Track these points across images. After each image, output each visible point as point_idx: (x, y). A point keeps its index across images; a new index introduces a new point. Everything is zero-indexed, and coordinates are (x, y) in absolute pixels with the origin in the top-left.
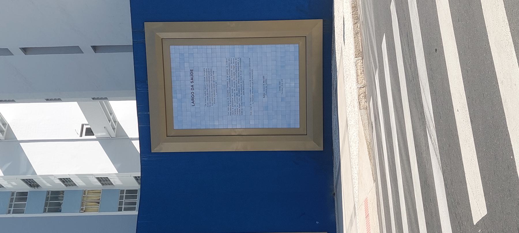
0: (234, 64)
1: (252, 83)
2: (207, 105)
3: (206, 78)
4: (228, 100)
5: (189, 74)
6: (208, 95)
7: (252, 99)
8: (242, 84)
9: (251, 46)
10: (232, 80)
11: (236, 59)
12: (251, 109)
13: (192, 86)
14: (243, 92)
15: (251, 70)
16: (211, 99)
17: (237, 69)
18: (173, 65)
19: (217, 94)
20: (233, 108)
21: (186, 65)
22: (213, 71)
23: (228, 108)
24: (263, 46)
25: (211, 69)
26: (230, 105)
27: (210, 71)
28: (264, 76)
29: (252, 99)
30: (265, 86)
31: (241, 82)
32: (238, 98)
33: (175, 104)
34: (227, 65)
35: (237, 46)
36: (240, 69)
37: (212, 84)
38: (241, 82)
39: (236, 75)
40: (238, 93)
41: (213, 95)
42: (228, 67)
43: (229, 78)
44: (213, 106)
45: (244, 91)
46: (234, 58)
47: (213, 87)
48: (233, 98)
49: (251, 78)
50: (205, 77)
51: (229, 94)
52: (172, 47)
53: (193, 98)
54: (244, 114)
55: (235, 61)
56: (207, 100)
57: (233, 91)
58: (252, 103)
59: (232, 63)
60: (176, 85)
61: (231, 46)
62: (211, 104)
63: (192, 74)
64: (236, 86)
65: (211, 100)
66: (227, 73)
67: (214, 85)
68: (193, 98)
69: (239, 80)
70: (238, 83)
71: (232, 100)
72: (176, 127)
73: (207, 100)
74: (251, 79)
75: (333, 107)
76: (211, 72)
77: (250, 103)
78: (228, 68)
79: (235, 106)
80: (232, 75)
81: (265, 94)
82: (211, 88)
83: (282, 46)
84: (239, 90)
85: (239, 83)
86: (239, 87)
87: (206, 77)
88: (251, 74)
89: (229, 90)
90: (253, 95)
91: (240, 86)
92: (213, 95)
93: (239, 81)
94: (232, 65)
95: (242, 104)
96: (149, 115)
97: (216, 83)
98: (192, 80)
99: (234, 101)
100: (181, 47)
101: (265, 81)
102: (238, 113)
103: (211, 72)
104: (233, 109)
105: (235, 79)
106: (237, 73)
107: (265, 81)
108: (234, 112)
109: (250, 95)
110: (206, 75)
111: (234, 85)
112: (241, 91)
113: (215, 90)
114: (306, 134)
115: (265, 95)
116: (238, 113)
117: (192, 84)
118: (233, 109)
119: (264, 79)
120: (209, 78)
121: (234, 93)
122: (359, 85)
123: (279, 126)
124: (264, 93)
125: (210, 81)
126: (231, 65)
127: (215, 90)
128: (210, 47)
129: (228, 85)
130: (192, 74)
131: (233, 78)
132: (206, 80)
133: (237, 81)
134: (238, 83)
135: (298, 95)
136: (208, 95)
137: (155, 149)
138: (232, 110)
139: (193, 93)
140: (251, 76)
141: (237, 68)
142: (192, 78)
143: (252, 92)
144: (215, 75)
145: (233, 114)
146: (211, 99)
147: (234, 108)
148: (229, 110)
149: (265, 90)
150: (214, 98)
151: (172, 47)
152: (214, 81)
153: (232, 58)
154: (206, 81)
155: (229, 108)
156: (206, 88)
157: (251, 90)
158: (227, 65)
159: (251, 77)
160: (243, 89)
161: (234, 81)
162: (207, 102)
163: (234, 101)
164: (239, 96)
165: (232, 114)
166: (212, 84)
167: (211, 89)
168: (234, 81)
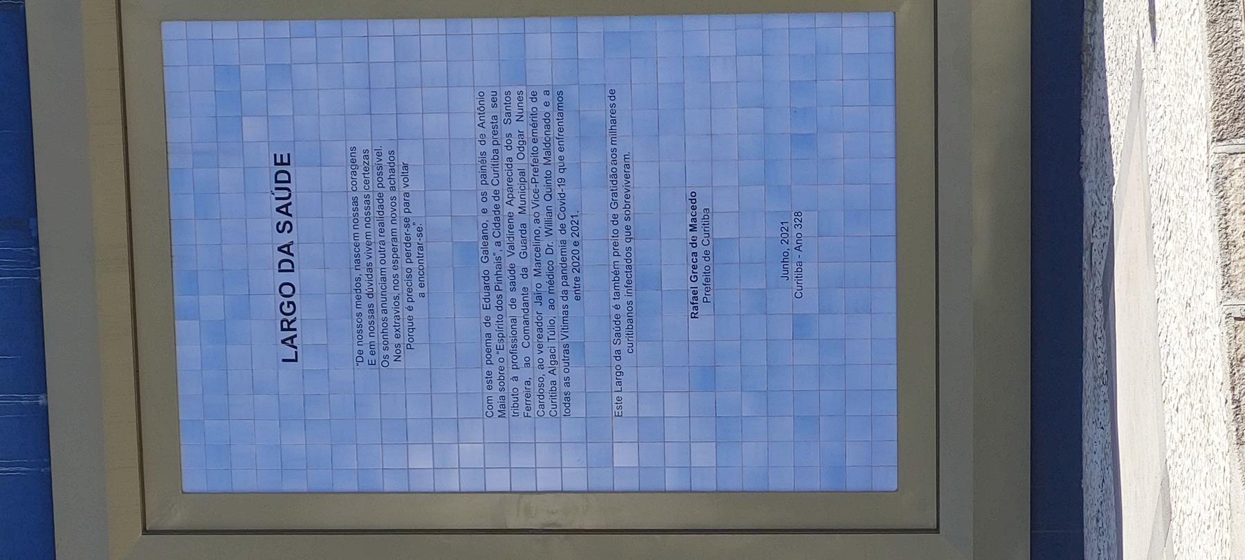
0: (524, 126)
2: (367, 355)
3: (362, 205)
4: (486, 330)
5: (267, 182)
6: (373, 301)
7: (624, 325)
8: (567, 237)
9: (621, 24)
11: (534, 94)
12: (619, 383)
13: (285, 249)
14: (571, 281)
15: (620, 159)
16: (391, 322)
17: (542, 154)
18: (180, 130)
19: (422, 295)
21: (253, 128)
22: (406, 166)
23: (489, 373)
26: (501, 360)
27: (385, 161)
28: (694, 194)
29: (624, 325)
30: (700, 250)
31: (563, 227)
32: (547, 315)
33: (189, 351)
34: (481, 131)
35: (543, 22)
37: (395, 239)
38: (563, 227)
40: (545, 287)
41: (404, 303)
43: (491, 203)
44: (400, 365)
45: (577, 279)
46: (523, 89)
47: (402, 253)
48: (514, 320)
49: (622, 203)
50: (355, 201)
51: (494, 295)
53: (290, 318)
55: (528, 106)
56: (366, 331)
57: (519, 279)
58: (624, 345)
59: (514, 118)
61: (505, 25)
62: (392, 352)
63: (282, 182)
64: (531, 250)
65: (391, 331)
66: (484, 176)
68: (290, 318)
69: (549, 212)
70: (543, 234)
71: (508, 332)
72: (193, 481)
73: (366, 331)
74: (620, 212)
75: (1088, 374)
76: (392, 170)
77: (617, 347)
78: (489, 148)
79: (527, 364)
80: (510, 189)
81: (701, 295)
82: (389, 259)
83: (799, 22)
84: (551, 274)
85: (549, 233)
86: (550, 258)
87: (361, 201)
88: (621, 179)
89: (493, 271)
91: (558, 250)
92: (404, 303)
93: (549, 223)
94: (514, 128)
95: (567, 351)
96: (45, 409)
97: (420, 230)
98: (287, 213)
99: (520, 335)
100: (226, 30)
101: (699, 220)
102: (542, 406)
103: (392, 170)
104: (515, 378)
105: (529, 210)
106: (542, 173)
107: (699, 220)
108: (522, 398)
109: (614, 303)
110: (360, 185)
112: (565, 277)
114: (933, 525)
115: (700, 303)
116: (542, 406)
117: (285, 238)
118: (515, 378)
119: (694, 208)
120: (381, 206)
121: (519, 287)
122: (1234, 301)
123: (784, 480)
124: (695, 293)
125: (387, 222)
126: (505, 129)
129: (485, 245)
130: (282, 182)
131: (517, 202)
132: (362, 213)
133: (537, 221)
134: (543, 234)
135: (887, 302)
136: (373, 301)
139: (287, 290)
141: (540, 145)
142: (286, 206)
143: (623, 282)
144: (416, 184)
146: (391, 322)
147: (524, 374)
148: (496, 384)
150: (410, 319)
153: (514, 91)
154: (362, 223)
155: (496, 376)
156: (364, 260)
159: (621, 199)
161: (523, 219)
162: (367, 340)
163: (520, 335)
164: (552, 306)
165: (509, 411)
166: (395, 239)
167: (389, 264)
168: (523, 219)
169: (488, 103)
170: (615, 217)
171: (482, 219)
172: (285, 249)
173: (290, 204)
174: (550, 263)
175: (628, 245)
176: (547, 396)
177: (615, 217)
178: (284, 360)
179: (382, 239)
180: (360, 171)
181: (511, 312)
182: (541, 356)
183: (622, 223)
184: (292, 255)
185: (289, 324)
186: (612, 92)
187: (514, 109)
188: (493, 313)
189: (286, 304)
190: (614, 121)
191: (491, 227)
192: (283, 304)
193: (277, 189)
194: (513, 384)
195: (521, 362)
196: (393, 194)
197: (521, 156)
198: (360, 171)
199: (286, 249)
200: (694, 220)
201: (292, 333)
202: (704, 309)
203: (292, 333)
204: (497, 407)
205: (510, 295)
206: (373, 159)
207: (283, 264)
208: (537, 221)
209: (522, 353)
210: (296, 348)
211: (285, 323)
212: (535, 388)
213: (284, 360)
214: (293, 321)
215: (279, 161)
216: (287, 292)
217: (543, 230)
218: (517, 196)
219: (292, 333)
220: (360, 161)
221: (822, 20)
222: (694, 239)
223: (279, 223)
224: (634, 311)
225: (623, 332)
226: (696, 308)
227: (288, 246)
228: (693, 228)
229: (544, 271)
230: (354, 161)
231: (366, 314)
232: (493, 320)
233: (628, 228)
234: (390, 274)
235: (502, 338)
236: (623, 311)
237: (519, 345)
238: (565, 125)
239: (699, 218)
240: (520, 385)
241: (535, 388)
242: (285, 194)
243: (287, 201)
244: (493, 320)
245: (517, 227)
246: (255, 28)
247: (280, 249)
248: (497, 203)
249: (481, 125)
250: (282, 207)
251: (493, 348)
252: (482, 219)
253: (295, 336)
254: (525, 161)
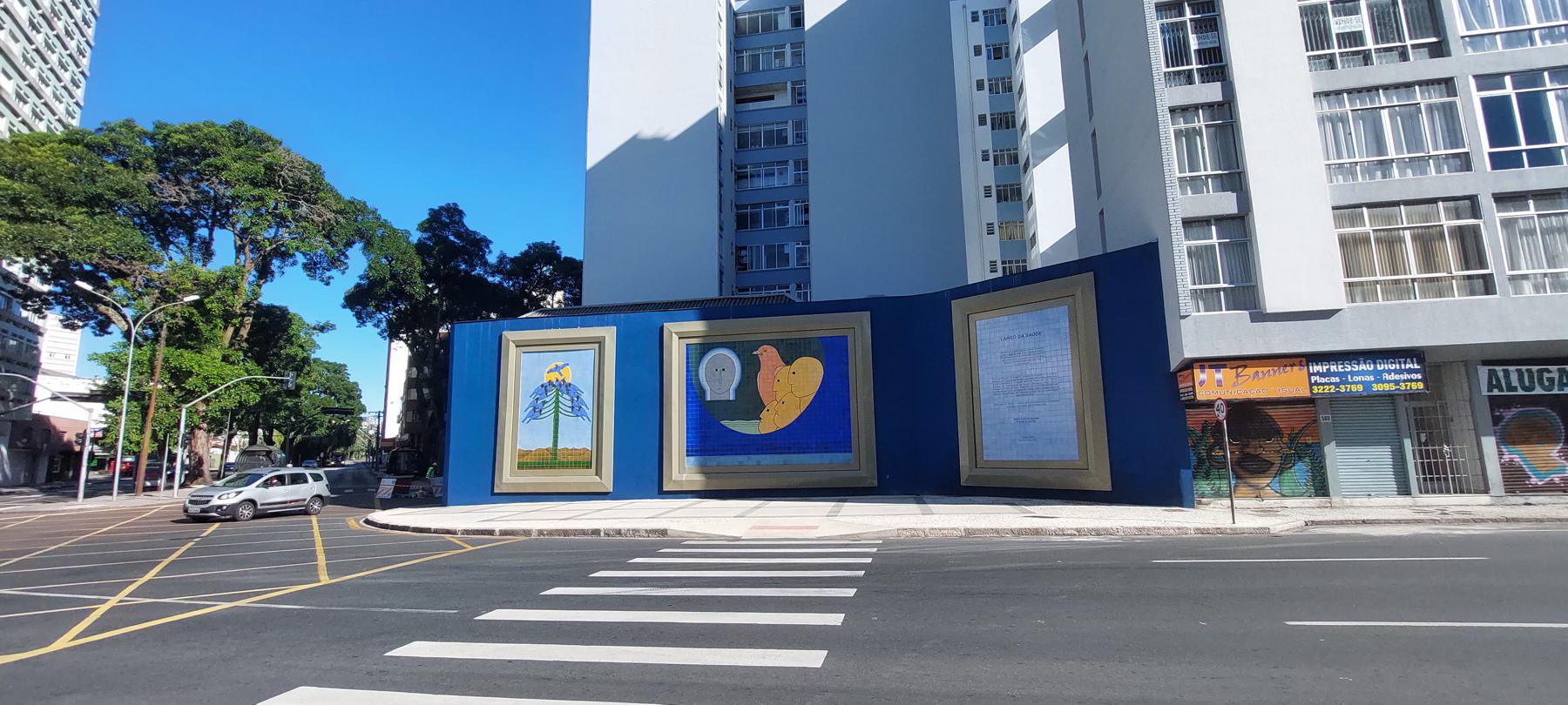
107: (1033, 420)
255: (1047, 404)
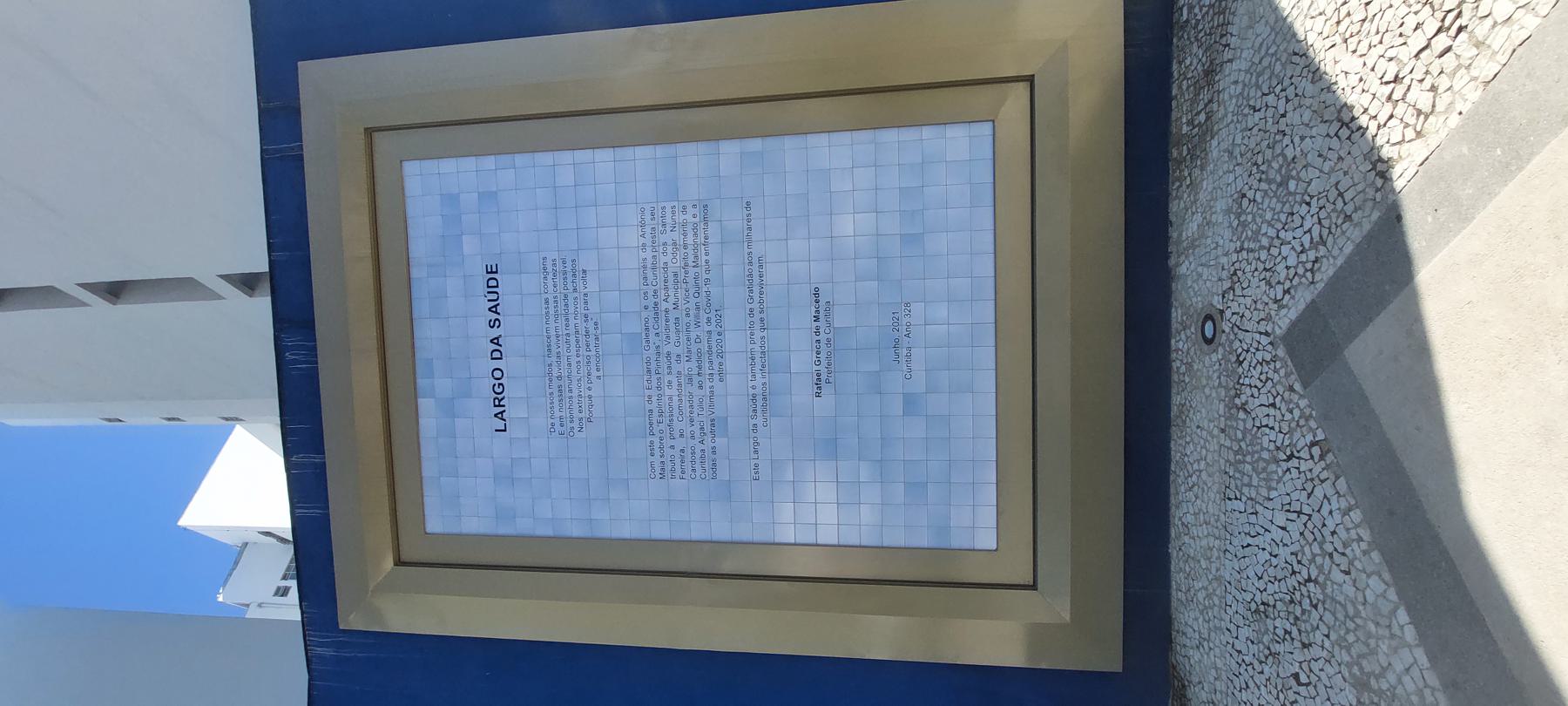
0: (676, 236)
1: (757, 326)
3: (551, 305)
4: (648, 407)
5: (481, 288)
6: (562, 383)
9: (755, 145)
10: (667, 311)
12: (756, 452)
13: (495, 341)
14: (716, 366)
15: (755, 260)
16: (575, 400)
17: (691, 258)
18: (420, 248)
19: (599, 377)
20: (672, 442)
21: (469, 245)
22: (584, 271)
23: (652, 442)
24: (813, 140)
25: (573, 261)
26: (661, 431)
27: (569, 269)
30: (823, 337)
31: (709, 320)
33: (429, 421)
34: (642, 240)
35: (692, 147)
36: (704, 258)
37: (577, 332)
38: (709, 320)
39: (684, 286)
40: (695, 371)
41: (584, 383)
42: (649, 249)
43: (652, 300)
44: (582, 435)
45: (721, 364)
46: (676, 203)
47: (582, 343)
48: (671, 398)
49: (757, 299)
50: (547, 302)
51: (654, 378)
52: (411, 168)
53: (500, 397)
54: (723, 474)
58: (759, 421)
59: (668, 228)
60: (430, 334)
61: (661, 151)
62: (576, 425)
63: (492, 288)
64: (683, 338)
65: (575, 407)
67: (587, 334)
68: (500, 397)
72: (434, 525)
73: (556, 409)
74: (756, 306)
76: (574, 275)
77: (754, 422)
78: (649, 254)
79: (682, 436)
80: (666, 288)
81: (823, 377)
82: (573, 349)
83: (908, 135)
85: (697, 325)
86: (699, 346)
89: (654, 358)
90: (766, 380)
91: (704, 338)
93: (697, 316)
94: (668, 237)
95: (713, 425)
97: (596, 324)
98: (496, 312)
99: (676, 412)
100: (448, 166)
101: (821, 310)
102: (694, 470)
103: (574, 275)
105: (682, 306)
107: (821, 310)
108: (678, 461)
109: (751, 384)
111: (678, 331)
113: (593, 360)
116: (694, 470)
117: (495, 332)
120: (566, 305)
121: (674, 371)
125: (571, 317)
127: (593, 360)
128: (566, 157)
130: (492, 288)
131: (672, 299)
132: (552, 311)
133: (688, 315)
134: (692, 327)
135: (987, 382)
136: (562, 383)
137: (352, 619)
138: (668, 451)
139: (497, 375)
140: (756, 289)
142: (496, 306)
143: (758, 367)
144: (592, 286)
145: (673, 470)
146: (575, 400)
147: (680, 443)
148: (657, 452)
149: (823, 356)
150: (590, 397)
151: (411, 168)
152: (586, 316)
154: (552, 319)
155: (657, 445)
157: (758, 360)
158: (642, 240)
159: (756, 295)
160: (721, 355)
162: (558, 414)
163: (676, 412)
164: (701, 387)
165: (668, 474)
166: (577, 332)
169: (648, 217)
170: (751, 310)
171: (645, 314)
172: (495, 341)
173: (498, 304)
174: (699, 352)
175: (762, 334)
176: (698, 461)
177: (751, 310)
178: (497, 430)
179: (568, 332)
180: (550, 276)
181: (668, 392)
182: (692, 428)
183: (757, 316)
184: (500, 346)
185: (500, 401)
186: (748, 203)
187: (669, 220)
188: (654, 392)
189: (497, 385)
190: (750, 228)
191: (651, 321)
192: (495, 385)
193: (489, 292)
194: (671, 452)
195: (677, 434)
196: (576, 295)
197: (674, 261)
198: (550, 276)
199: (496, 341)
200: (817, 311)
201: (502, 409)
202: (826, 389)
203: (502, 409)
204: (658, 470)
205: (667, 378)
206: (559, 267)
207: (494, 353)
208: (688, 315)
209: (677, 426)
210: (505, 420)
211: (497, 401)
212: (688, 457)
213: (497, 430)
214: (502, 399)
215: (489, 270)
216: (497, 375)
217: (692, 323)
218: (671, 293)
219: (502, 409)
220: (550, 269)
221: (927, 132)
222: (818, 328)
223: (491, 321)
224: (767, 391)
225: (759, 409)
226: (820, 388)
227: (497, 338)
228: (817, 319)
229: (694, 357)
230: (545, 268)
231: (556, 394)
232: (654, 399)
233: (762, 320)
234: (574, 360)
235: (661, 413)
236: (759, 391)
237: (674, 418)
238: (709, 232)
239: (822, 312)
240: (676, 453)
241: (688, 457)
242: (494, 297)
243: (496, 303)
244: (654, 399)
245: (672, 321)
246: (469, 163)
247: (492, 341)
248: (656, 300)
249: (643, 236)
250: (492, 307)
251: (655, 422)
252: (645, 314)
253: (504, 411)
254: (678, 264)
255: (757, 249)
